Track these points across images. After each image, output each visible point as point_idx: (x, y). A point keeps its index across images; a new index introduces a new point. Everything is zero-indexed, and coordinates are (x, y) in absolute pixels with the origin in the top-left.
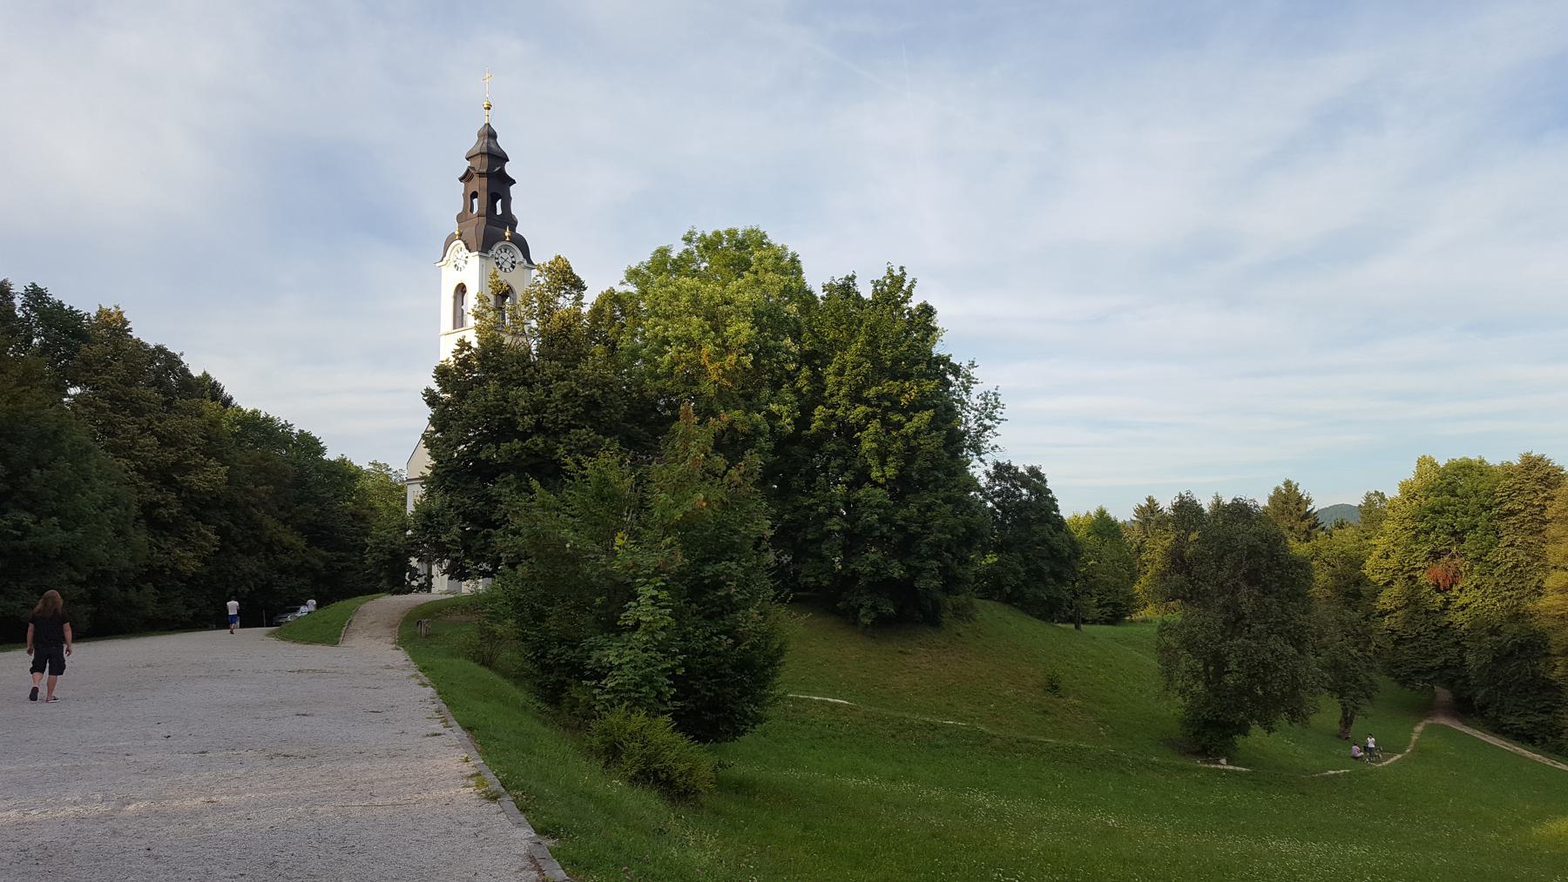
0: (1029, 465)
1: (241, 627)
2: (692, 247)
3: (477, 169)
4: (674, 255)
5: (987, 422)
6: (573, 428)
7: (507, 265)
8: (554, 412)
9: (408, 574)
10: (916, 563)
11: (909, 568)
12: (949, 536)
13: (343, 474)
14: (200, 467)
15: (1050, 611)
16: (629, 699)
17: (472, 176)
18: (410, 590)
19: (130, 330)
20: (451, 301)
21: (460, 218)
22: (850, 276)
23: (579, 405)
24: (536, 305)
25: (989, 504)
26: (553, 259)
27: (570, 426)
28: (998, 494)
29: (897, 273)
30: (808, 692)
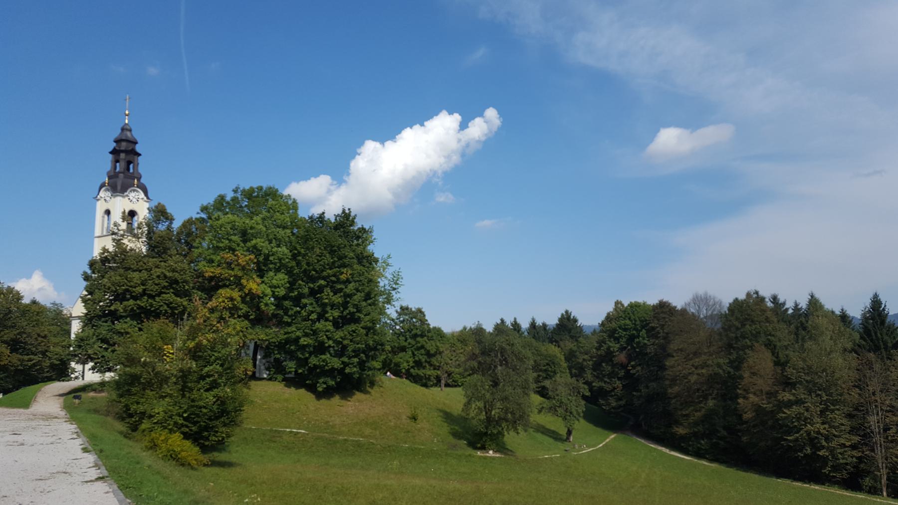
0: (417, 307)
2: (239, 195)
4: (228, 198)
5: (394, 286)
7: (134, 200)
10: (345, 359)
11: (343, 363)
12: (364, 346)
15: (424, 382)
20: (101, 218)
25: (398, 327)
27: (161, 293)
28: (402, 322)
29: (347, 211)
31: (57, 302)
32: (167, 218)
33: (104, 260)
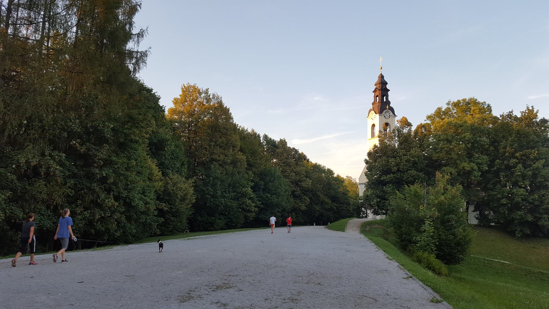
1: (316, 225)
2: (450, 106)
3: (378, 88)
4: (443, 110)
6: (409, 170)
8: (403, 166)
9: (362, 213)
10: (538, 216)
11: (535, 217)
13: (339, 180)
14: (305, 181)
16: (423, 249)
17: (377, 90)
18: (362, 217)
19: (287, 144)
21: (373, 104)
22: (511, 111)
23: (411, 163)
24: (397, 133)
26: (402, 118)
29: (531, 108)
30: (494, 258)
31: (349, 176)
32: (408, 126)
33: (376, 152)
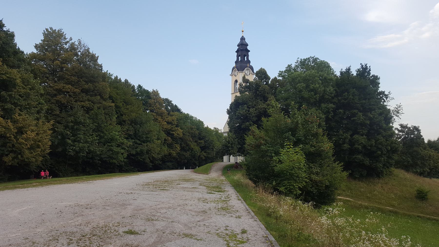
7: (248, 74)
21: (236, 62)
